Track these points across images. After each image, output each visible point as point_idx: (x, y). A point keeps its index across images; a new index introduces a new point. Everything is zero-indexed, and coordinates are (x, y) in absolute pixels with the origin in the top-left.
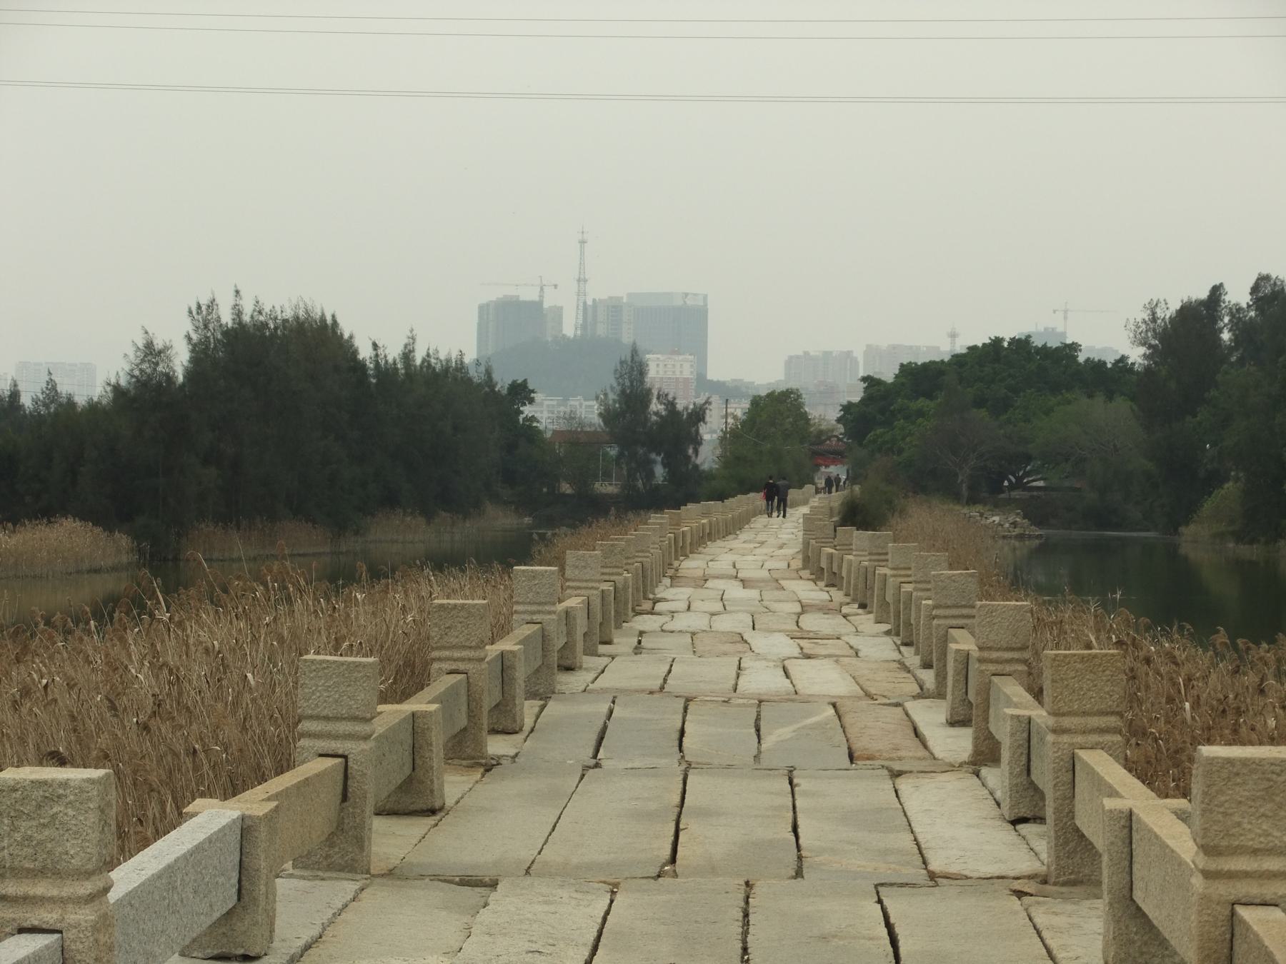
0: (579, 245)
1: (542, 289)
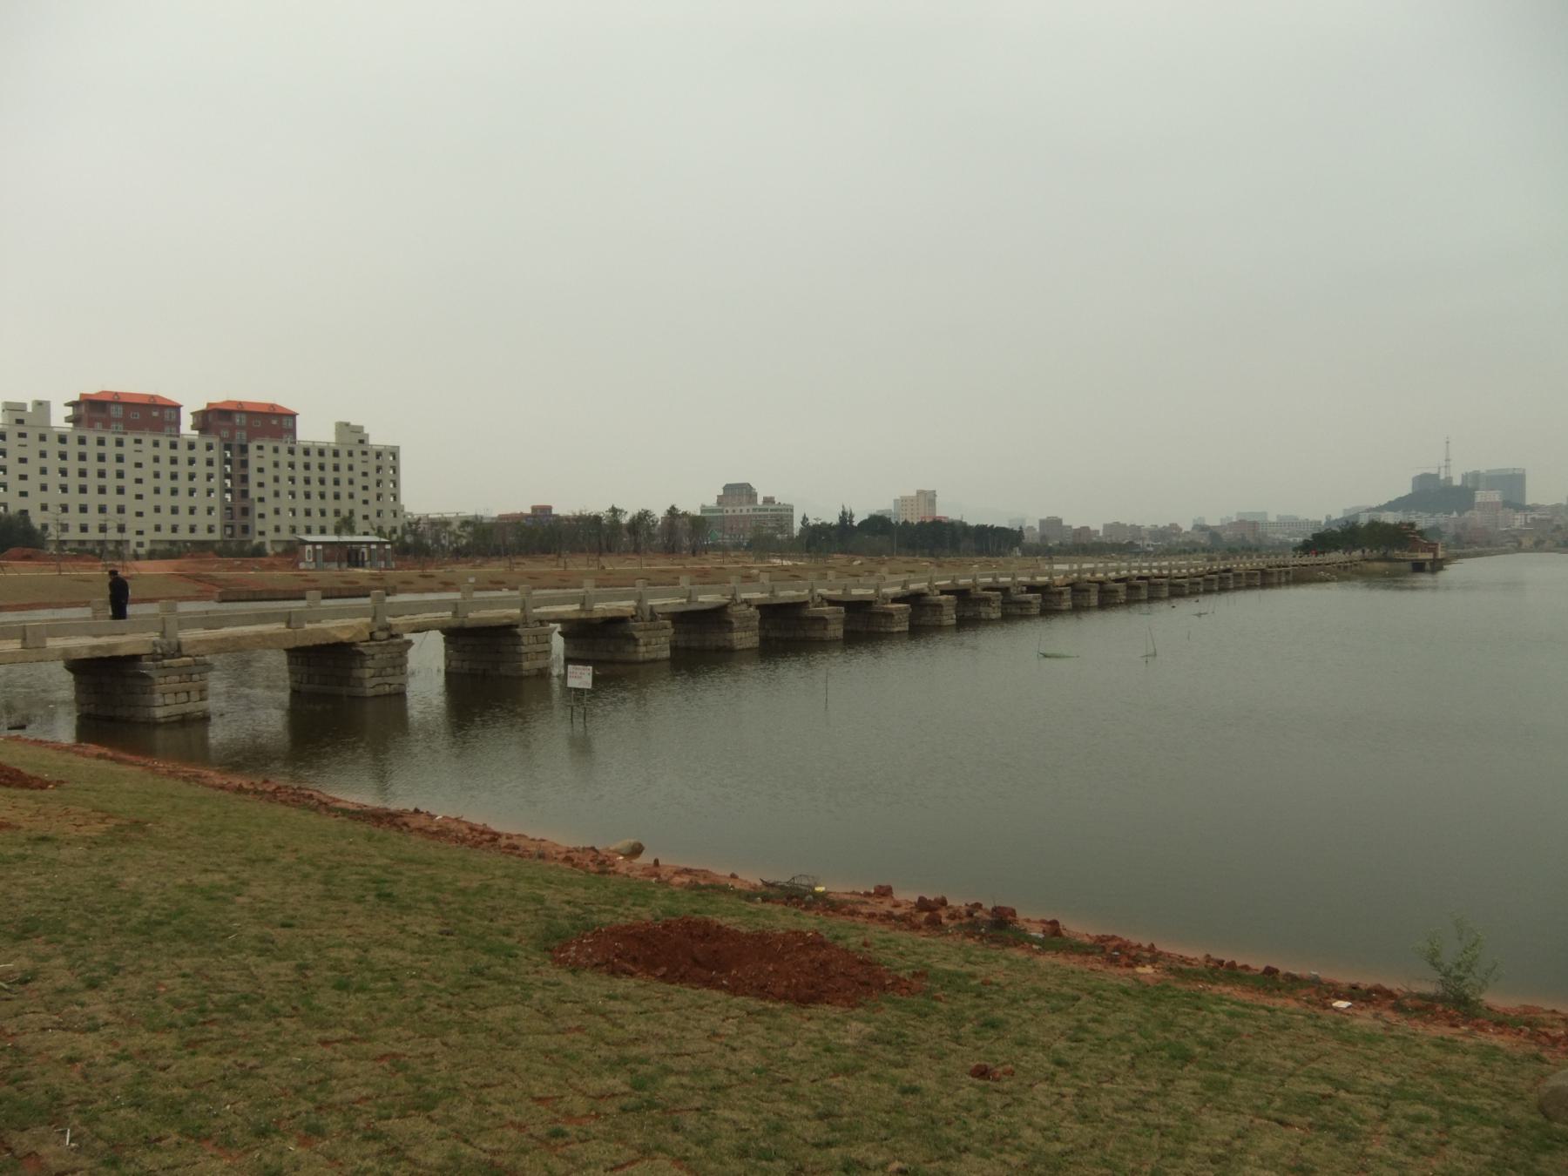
1: (1439, 468)
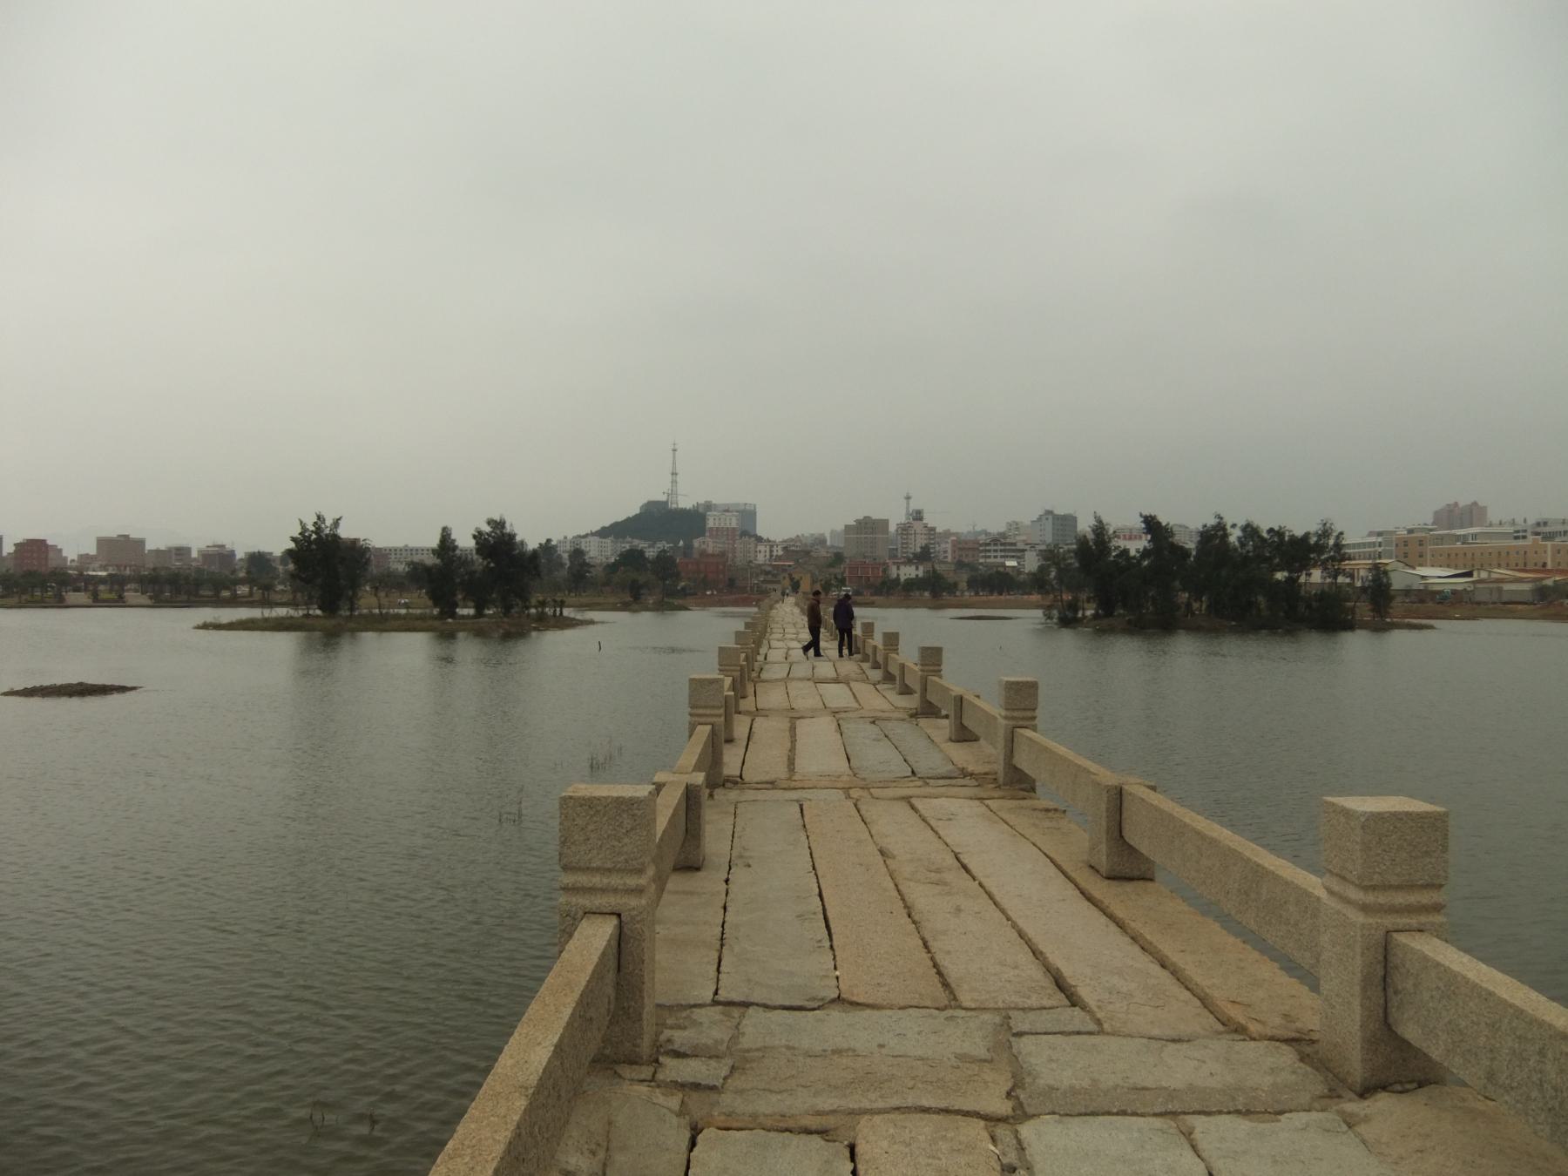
0: (672, 452)
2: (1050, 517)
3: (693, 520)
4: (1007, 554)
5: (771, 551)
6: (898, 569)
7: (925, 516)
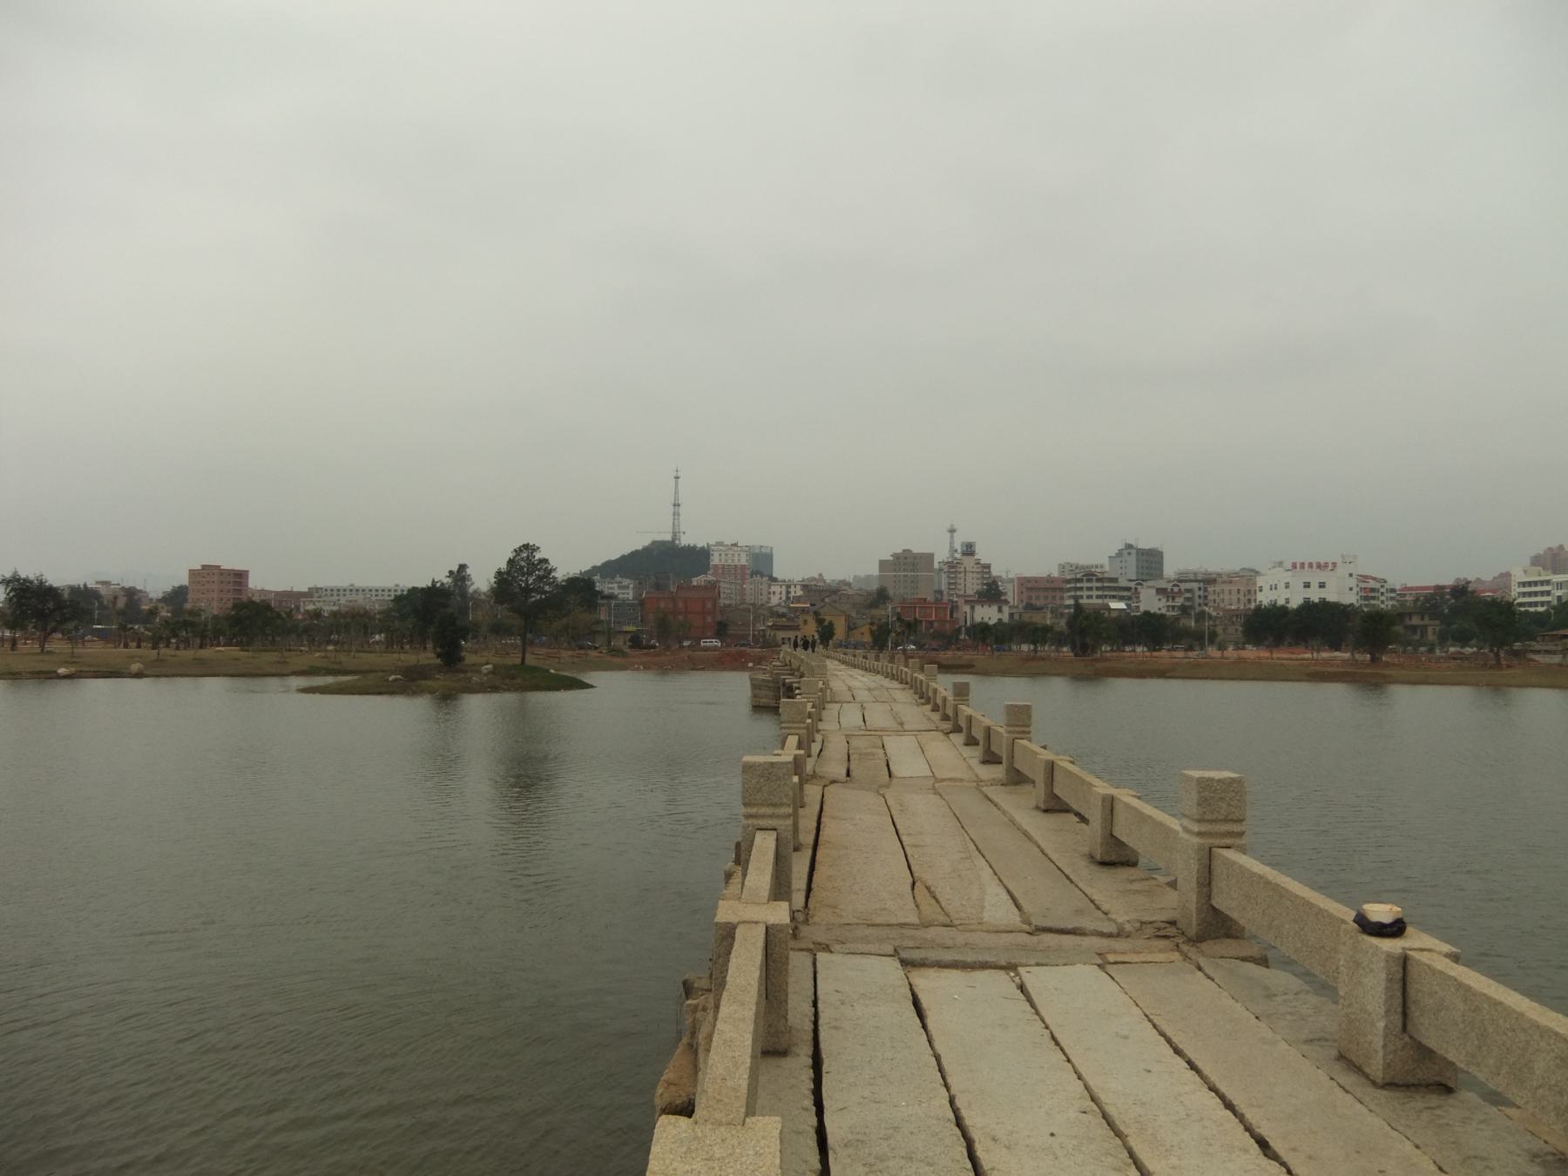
2: (1134, 552)
3: (698, 558)
4: (1106, 593)
5: (788, 593)
6: (973, 608)
7: (978, 549)
